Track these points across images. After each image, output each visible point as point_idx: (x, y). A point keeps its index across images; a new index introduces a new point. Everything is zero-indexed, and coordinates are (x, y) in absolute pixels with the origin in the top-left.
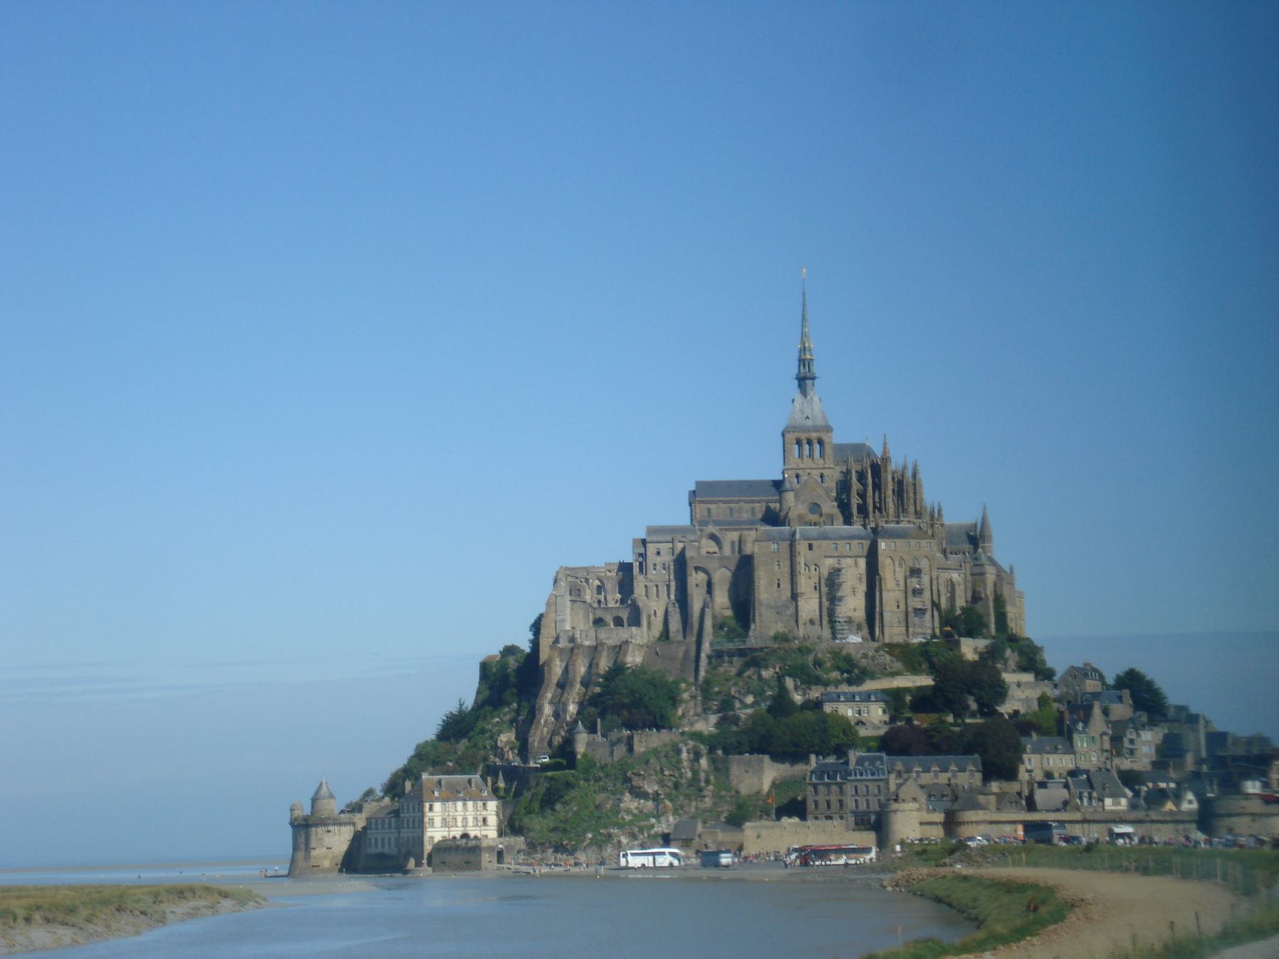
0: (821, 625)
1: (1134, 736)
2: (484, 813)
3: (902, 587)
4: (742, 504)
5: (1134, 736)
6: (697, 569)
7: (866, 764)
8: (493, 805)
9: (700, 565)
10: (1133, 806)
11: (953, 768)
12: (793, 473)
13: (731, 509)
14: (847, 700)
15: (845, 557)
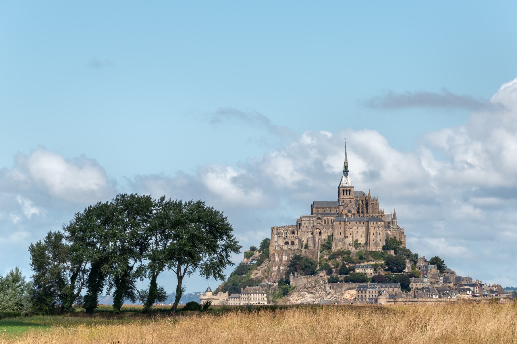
0: (352, 245)
1: (438, 278)
2: (264, 297)
3: (375, 235)
4: (327, 209)
5: (438, 278)
6: (316, 228)
7: (372, 286)
8: (265, 295)
9: (318, 227)
10: (440, 297)
11: (393, 287)
12: (342, 200)
13: (324, 210)
14: (362, 268)
15: (360, 226)
